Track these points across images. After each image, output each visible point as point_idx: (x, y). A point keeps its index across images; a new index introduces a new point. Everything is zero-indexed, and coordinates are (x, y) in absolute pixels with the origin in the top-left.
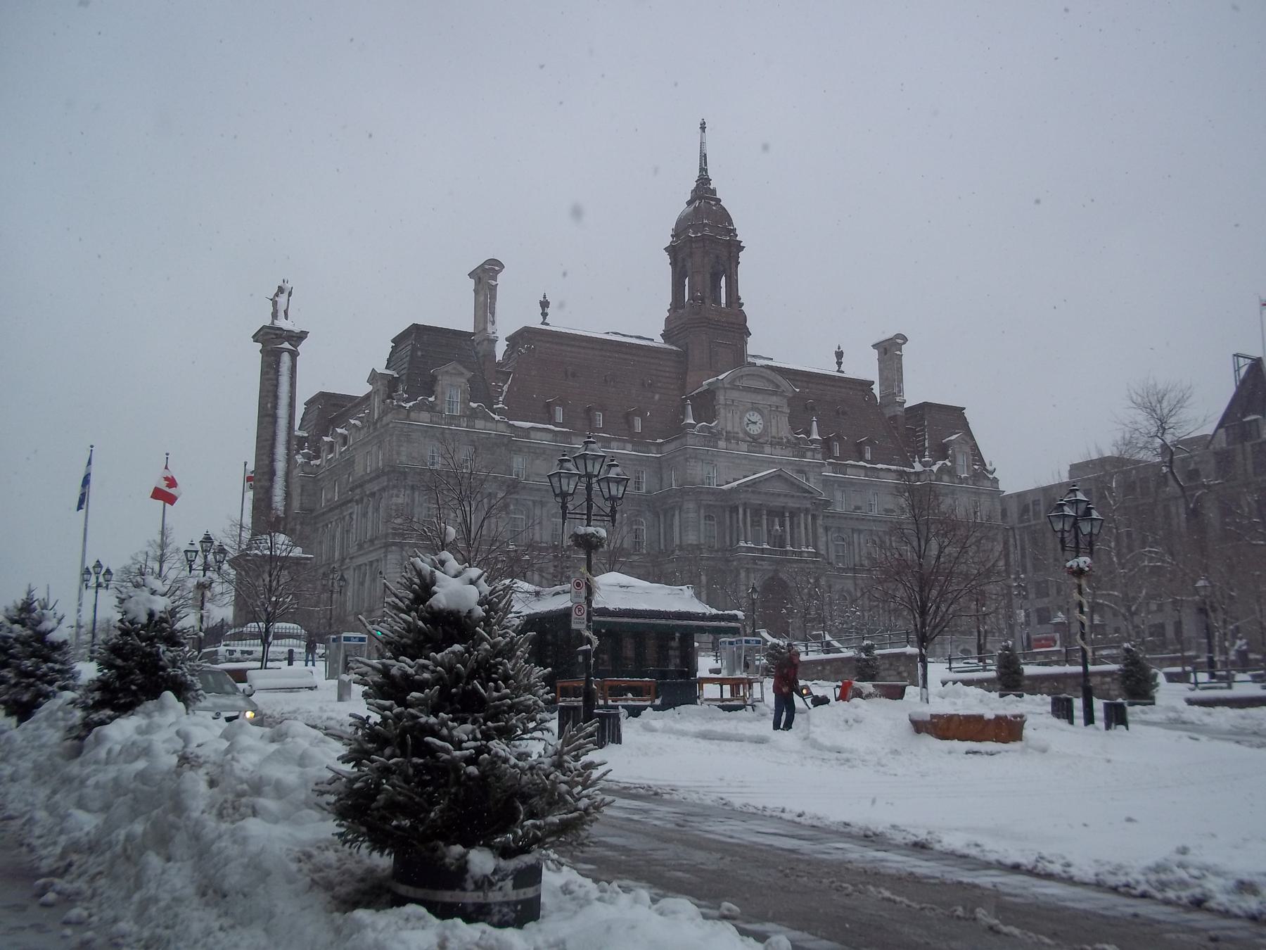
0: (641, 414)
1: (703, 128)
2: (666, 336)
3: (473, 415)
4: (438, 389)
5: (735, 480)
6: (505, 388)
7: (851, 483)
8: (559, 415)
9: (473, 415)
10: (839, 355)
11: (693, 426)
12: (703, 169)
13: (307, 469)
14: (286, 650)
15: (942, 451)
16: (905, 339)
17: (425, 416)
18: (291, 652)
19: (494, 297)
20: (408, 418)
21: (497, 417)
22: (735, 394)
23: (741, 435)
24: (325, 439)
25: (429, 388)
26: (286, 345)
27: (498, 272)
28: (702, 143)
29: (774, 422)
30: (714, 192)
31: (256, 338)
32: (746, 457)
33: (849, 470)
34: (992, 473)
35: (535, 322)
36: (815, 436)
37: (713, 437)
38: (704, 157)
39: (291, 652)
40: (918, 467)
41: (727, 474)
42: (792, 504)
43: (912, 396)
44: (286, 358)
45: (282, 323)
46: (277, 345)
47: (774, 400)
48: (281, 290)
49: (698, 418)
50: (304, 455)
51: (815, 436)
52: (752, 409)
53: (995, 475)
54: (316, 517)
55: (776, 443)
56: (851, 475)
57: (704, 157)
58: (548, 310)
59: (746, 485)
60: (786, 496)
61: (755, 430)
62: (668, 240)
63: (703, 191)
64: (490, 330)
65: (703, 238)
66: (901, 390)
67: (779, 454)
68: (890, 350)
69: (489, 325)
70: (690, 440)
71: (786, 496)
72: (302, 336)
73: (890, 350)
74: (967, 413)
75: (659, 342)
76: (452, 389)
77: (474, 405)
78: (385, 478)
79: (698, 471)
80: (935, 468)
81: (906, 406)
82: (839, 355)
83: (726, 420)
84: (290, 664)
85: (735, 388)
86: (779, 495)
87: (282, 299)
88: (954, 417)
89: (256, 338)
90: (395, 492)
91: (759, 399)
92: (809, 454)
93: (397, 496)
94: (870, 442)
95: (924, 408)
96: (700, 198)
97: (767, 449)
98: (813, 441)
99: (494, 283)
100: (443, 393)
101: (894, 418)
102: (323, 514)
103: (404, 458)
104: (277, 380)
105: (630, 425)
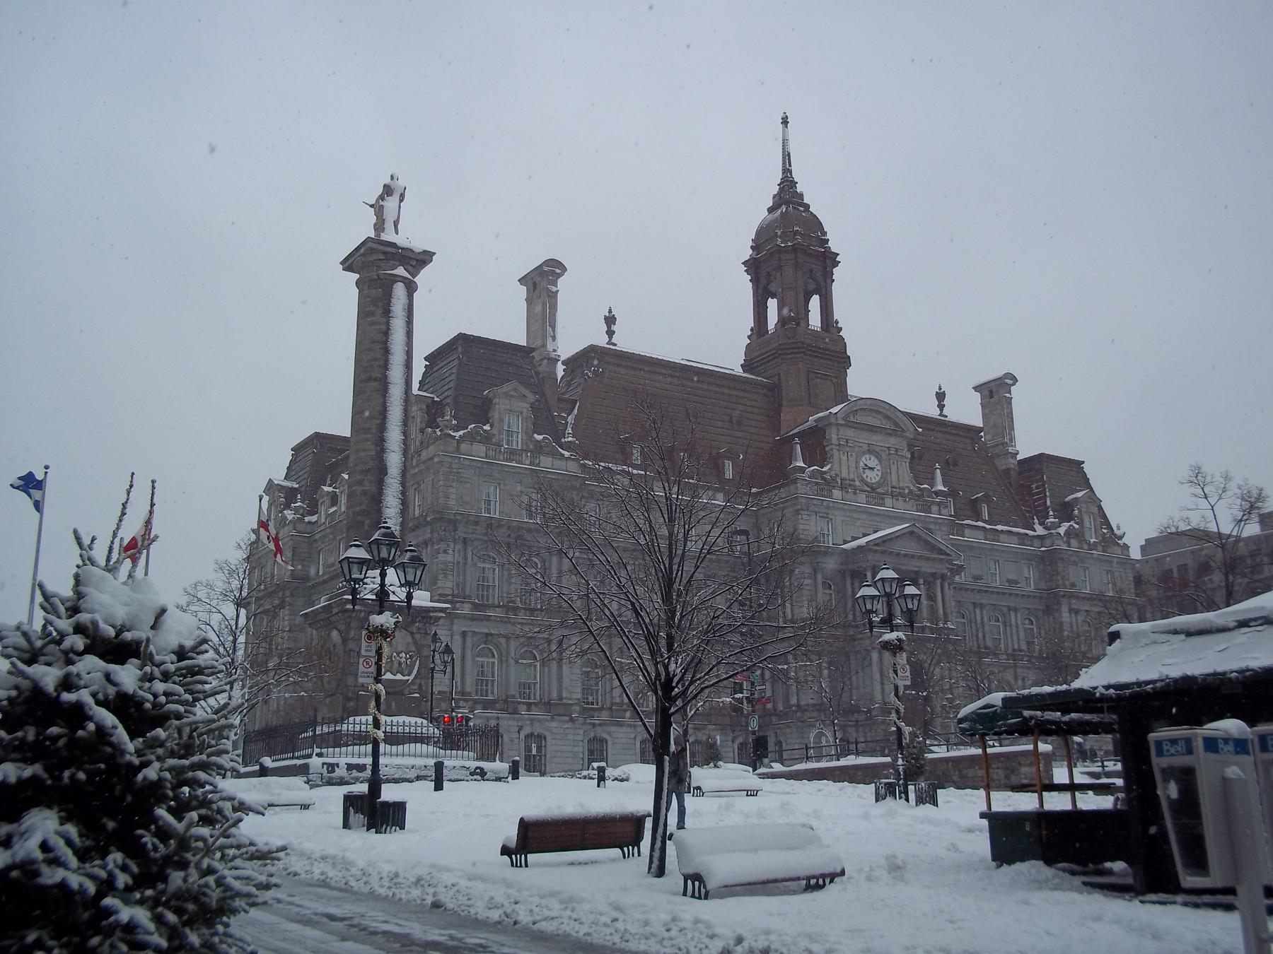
0: (731, 455)
1: (785, 122)
2: (747, 366)
3: (539, 449)
4: (496, 415)
5: (854, 539)
6: (571, 419)
7: (970, 547)
8: (636, 456)
9: (539, 449)
10: (941, 396)
11: (802, 470)
12: (787, 171)
13: (300, 527)
14: (432, 762)
15: (1066, 512)
16: (1015, 380)
17: (480, 449)
18: (439, 767)
19: (554, 307)
20: (458, 450)
21: (567, 454)
22: (850, 433)
23: (857, 483)
24: (326, 489)
25: (482, 412)
26: (400, 271)
27: (559, 276)
28: (785, 142)
29: (894, 468)
30: (801, 196)
31: (349, 264)
32: (865, 511)
33: (967, 532)
34: (1121, 538)
35: (602, 341)
36: (940, 487)
37: (827, 484)
38: (787, 156)
39: (439, 767)
40: (1040, 531)
41: (844, 530)
42: (927, 568)
43: (1026, 447)
44: (399, 290)
45: (389, 236)
46: (383, 270)
47: (893, 441)
48: (388, 191)
49: (809, 461)
50: (296, 510)
51: (940, 487)
52: (870, 452)
53: (1125, 540)
54: (313, 586)
55: (897, 494)
56: (970, 537)
57: (787, 156)
58: (614, 328)
59: (876, 543)
60: (920, 557)
61: (873, 477)
62: (747, 253)
63: (788, 195)
64: (550, 347)
65: (794, 249)
66: (1012, 439)
67: (901, 507)
68: (996, 393)
69: (549, 340)
70: (801, 488)
71: (920, 557)
72: (424, 259)
73: (996, 393)
74: (1087, 468)
75: (739, 371)
76: (512, 415)
77: (540, 437)
78: (428, 529)
79: (810, 526)
80: (1062, 530)
81: (1019, 457)
82: (941, 396)
83: (840, 465)
84: (438, 787)
85: (849, 425)
86: (913, 556)
87: (391, 204)
88: (1073, 471)
89: (349, 264)
90: (443, 546)
91: (878, 440)
92: (935, 508)
93: (445, 552)
94: (987, 499)
95: (1040, 461)
96: (787, 203)
97: (888, 501)
98: (938, 493)
99: (554, 289)
100: (501, 420)
101: (1007, 471)
102: (325, 582)
103: (452, 503)
104: (388, 324)
105: (720, 471)
